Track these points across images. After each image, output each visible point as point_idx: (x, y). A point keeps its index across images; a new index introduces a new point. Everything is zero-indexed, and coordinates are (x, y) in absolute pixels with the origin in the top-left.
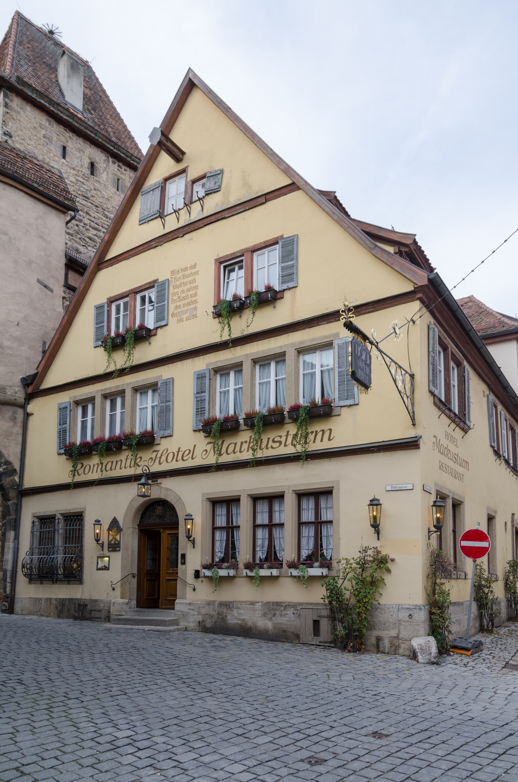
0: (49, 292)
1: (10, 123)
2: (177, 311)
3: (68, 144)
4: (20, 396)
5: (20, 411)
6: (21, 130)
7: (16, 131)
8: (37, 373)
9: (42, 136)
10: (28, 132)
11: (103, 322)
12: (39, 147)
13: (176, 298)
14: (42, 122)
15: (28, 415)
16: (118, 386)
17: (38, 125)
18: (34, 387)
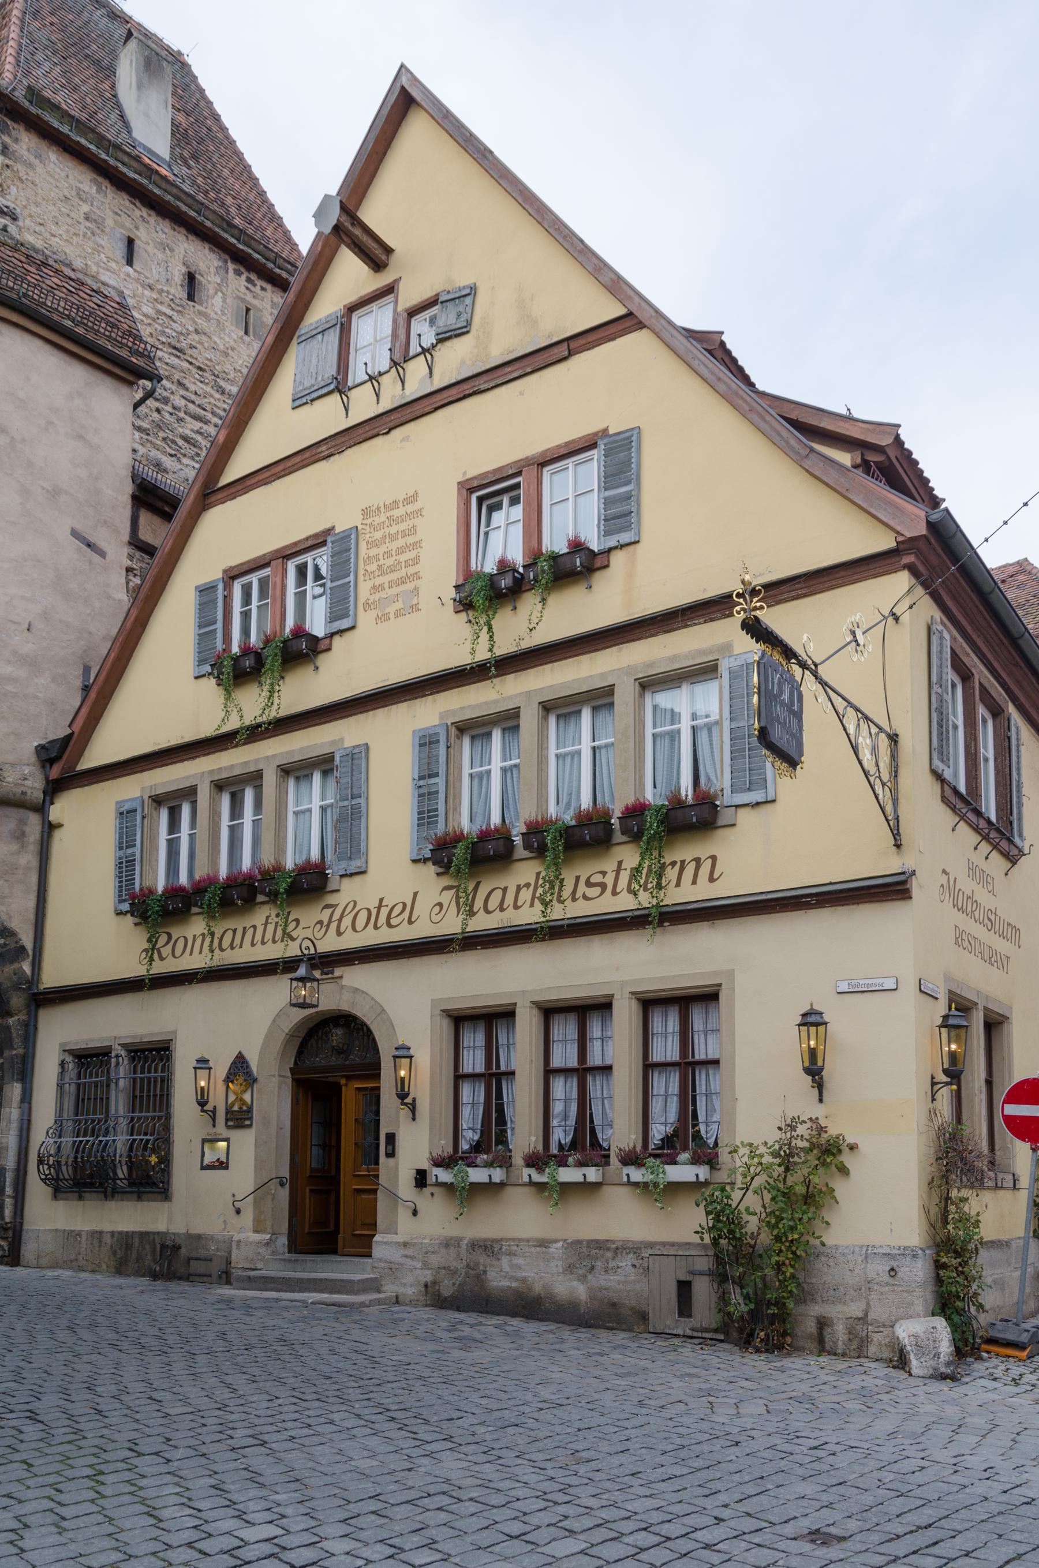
0: (96, 558)
1: (13, 190)
2: (376, 597)
3: (138, 233)
4: (34, 785)
5: (34, 820)
6: (37, 204)
7: (25, 207)
8: (71, 735)
9: (82, 216)
10: (52, 208)
11: (215, 623)
12: (75, 240)
13: (372, 567)
14: (81, 186)
15: (50, 828)
16: (246, 763)
17: (74, 193)
18: (63, 765)
